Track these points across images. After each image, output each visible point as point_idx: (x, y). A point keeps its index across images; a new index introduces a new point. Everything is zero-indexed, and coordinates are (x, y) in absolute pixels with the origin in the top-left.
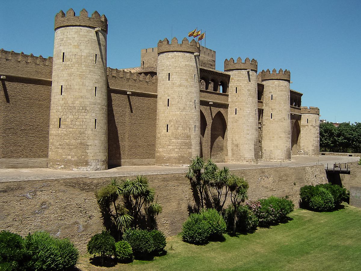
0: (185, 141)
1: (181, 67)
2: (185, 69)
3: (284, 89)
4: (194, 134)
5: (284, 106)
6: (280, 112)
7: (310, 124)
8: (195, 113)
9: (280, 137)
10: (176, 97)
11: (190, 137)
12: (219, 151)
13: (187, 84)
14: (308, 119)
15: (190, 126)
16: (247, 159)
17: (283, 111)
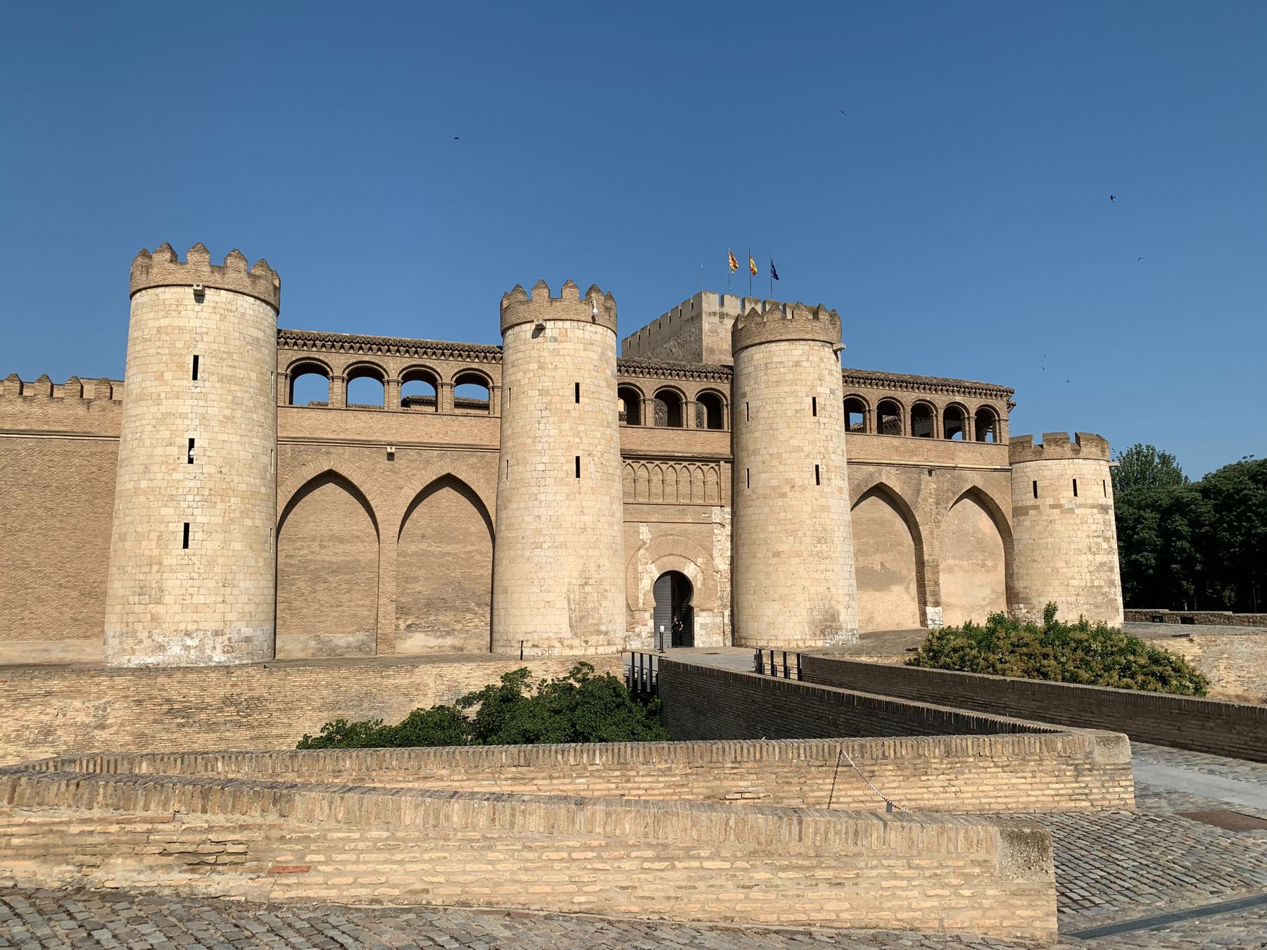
0: (141, 577)
1: (146, 340)
2: (158, 344)
3: (789, 377)
4: (183, 551)
5: (791, 438)
6: (775, 462)
7: (1046, 501)
8: (192, 484)
9: (777, 554)
10: (130, 436)
11: (160, 564)
12: (468, 610)
13: (159, 389)
14: (1035, 483)
15: (162, 528)
16: (536, 637)
17: (786, 456)
